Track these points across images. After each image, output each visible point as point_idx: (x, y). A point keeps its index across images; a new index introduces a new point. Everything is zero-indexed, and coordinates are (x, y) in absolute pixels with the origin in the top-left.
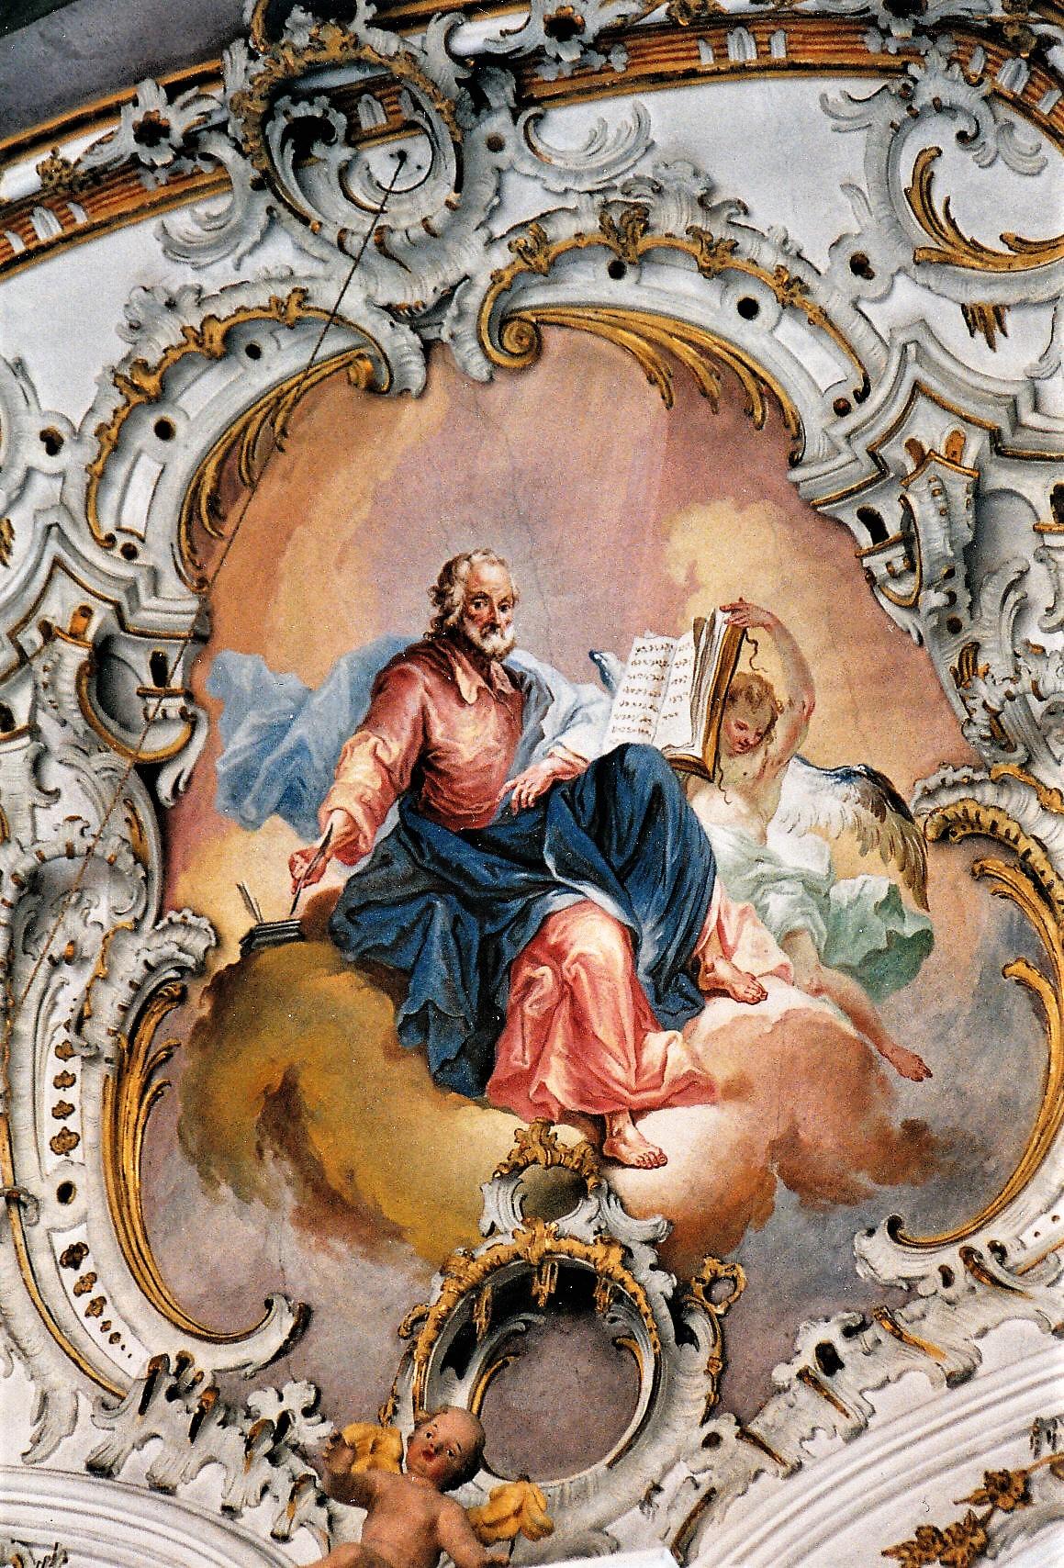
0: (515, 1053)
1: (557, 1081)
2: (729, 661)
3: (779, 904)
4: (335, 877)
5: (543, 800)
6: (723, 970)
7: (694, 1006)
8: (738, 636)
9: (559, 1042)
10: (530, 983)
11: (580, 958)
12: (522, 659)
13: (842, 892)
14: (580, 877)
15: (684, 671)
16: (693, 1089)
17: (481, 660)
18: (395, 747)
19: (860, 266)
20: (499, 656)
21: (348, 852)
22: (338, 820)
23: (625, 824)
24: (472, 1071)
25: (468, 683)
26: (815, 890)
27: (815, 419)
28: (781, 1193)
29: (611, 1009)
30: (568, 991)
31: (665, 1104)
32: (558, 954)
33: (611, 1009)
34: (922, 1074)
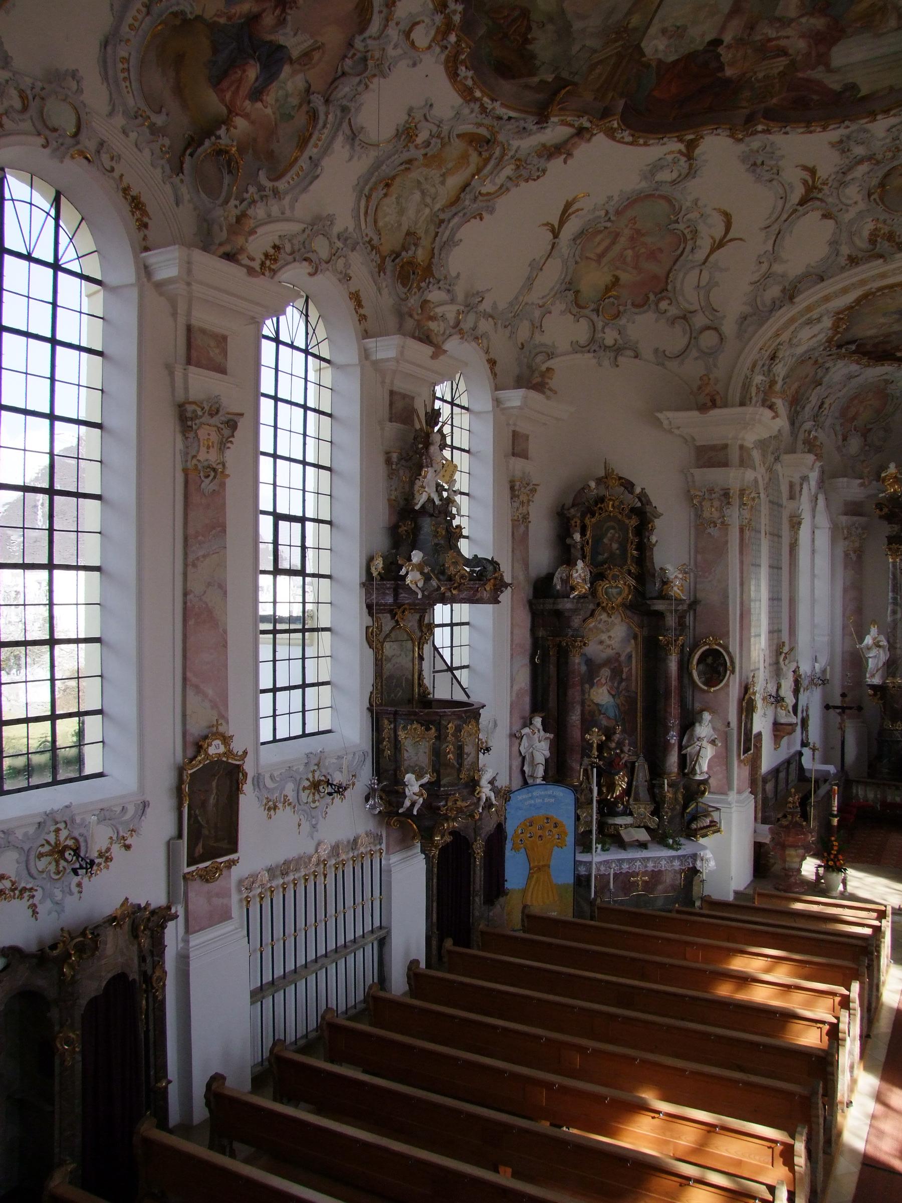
0: (225, 84)
1: (228, 96)
2: (314, 50)
3: (281, 93)
4: (222, 21)
5: (267, 42)
6: (264, 98)
7: (256, 101)
8: (319, 48)
9: (233, 88)
10: (236, 72)
11: (247, 76)
12: (289, 18)
13: (290, 99)
14: (259, 60)
15: (306, 45)
16: (246, 116)
17: (283, 11)
18: (256, 9)
19: (397, 24)
20: (287, 14)
21: (229, 18)
22: (233, 11)
23: (273, 58)
24: (217, 81)
25: (278, 12)
26: (287, 96)
27: (366, 34)
28: (251, 151)
29: (244, 90)
30: (240, 81)
31: (242, 116)
32: (244, 71)
33: (244, 90)
34: (278, 142)
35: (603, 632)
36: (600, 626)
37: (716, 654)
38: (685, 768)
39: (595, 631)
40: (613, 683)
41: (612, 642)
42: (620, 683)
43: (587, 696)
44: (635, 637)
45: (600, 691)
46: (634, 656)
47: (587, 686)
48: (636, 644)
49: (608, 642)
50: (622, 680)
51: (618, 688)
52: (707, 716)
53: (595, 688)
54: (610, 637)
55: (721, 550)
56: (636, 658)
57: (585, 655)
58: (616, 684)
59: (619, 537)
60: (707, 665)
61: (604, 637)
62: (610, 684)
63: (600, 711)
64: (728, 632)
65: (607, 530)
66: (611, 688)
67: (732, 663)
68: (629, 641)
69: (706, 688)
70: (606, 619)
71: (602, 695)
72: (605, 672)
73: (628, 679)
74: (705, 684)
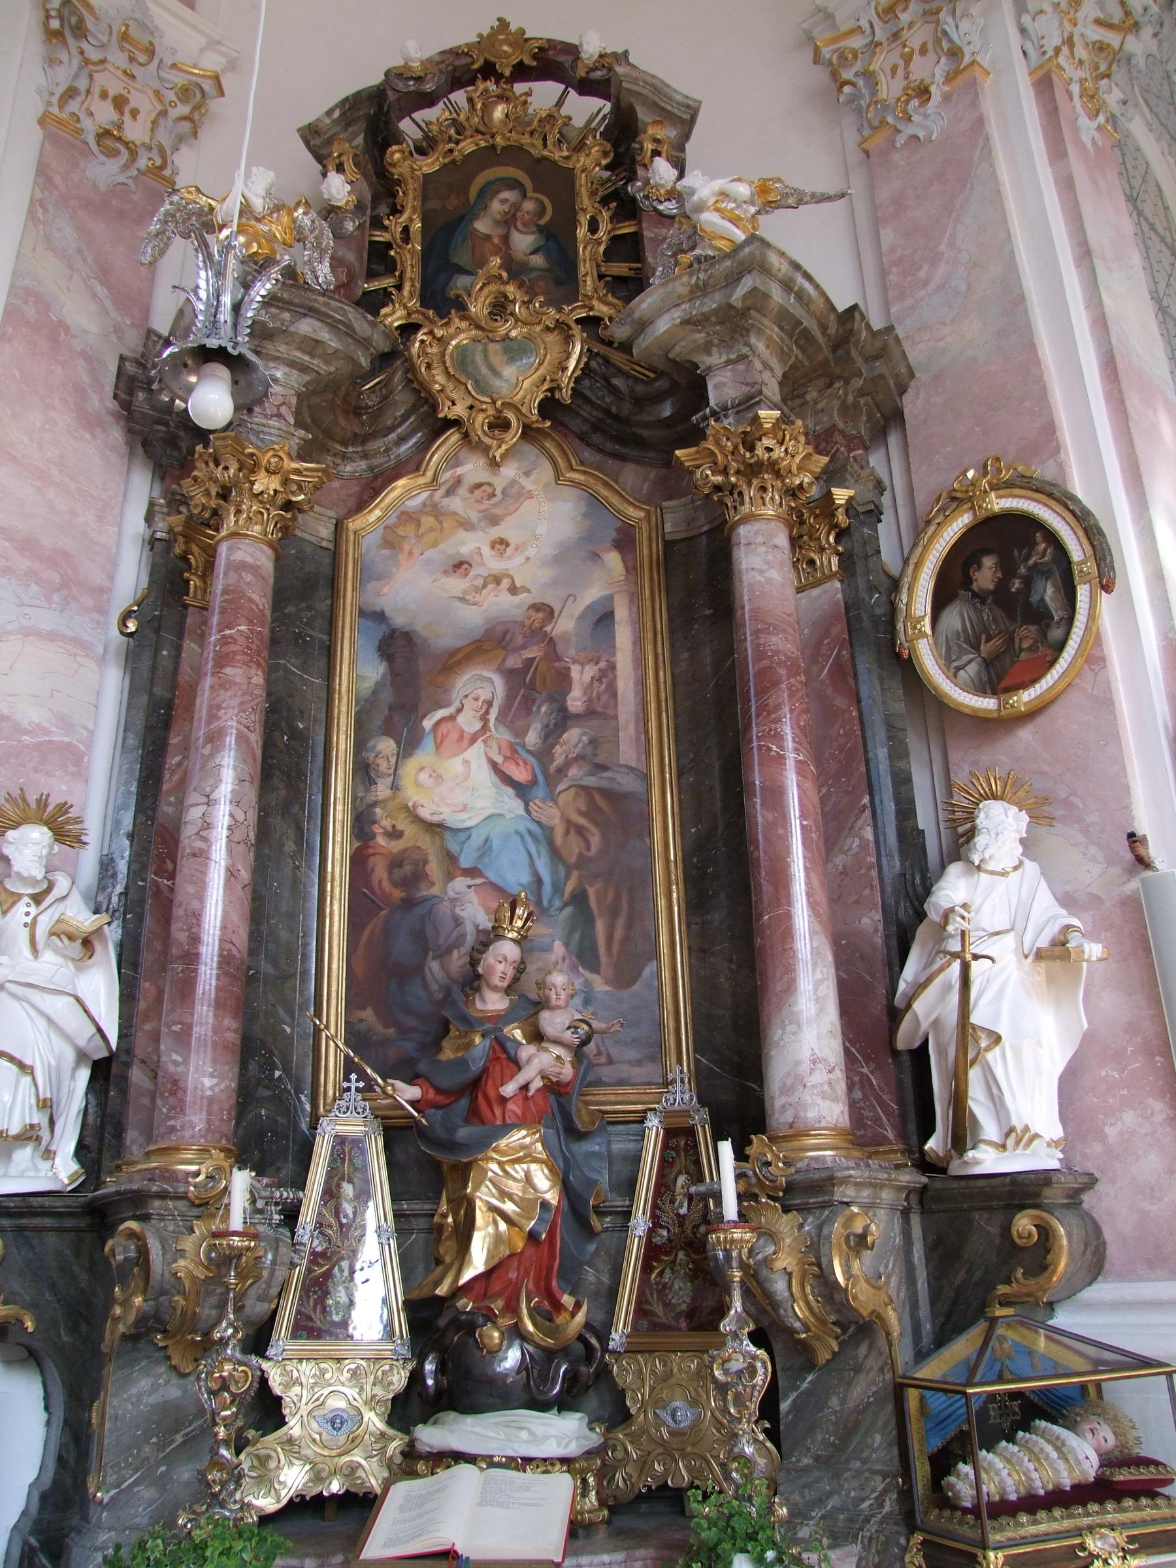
35: (467, 525)
36: (456, 504)
37: (1007, 536)
38: (927, 1129)
39: (428, 521)
40: (521, 733)
41: (511, 564)
42: (552, 733)
43: (382, 790)
44: (625, 541)
45: (454, 766)
46: (622, 613)
47: (386, 746)
48: (631, 568)
49: (493, 563)
50: (563, 719)
51: (544, 754)
52: (1002, 827)
53: (424, 756)
54: (501, 544)
55: (962, 164)
56: (638, 623)
57: (380, 617)
58: (533, 738)
59: (542, 212)
60: (980, 597)
61: (468, 544)
62: (502, 735)
63: (451, 859)
64: (1050, 429)
65: (489, 191)
66: (513, 753)
67: (1092, 532)
68: (595, 556)
69: (987, 704)
70: (483, 476)
71: (460, 783)
72: (479, 688)
73: (599, 712)
74: (995, 680)
